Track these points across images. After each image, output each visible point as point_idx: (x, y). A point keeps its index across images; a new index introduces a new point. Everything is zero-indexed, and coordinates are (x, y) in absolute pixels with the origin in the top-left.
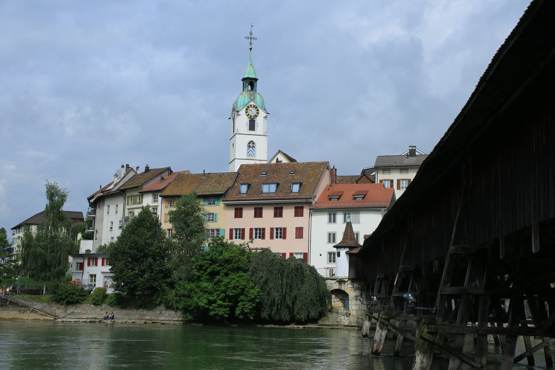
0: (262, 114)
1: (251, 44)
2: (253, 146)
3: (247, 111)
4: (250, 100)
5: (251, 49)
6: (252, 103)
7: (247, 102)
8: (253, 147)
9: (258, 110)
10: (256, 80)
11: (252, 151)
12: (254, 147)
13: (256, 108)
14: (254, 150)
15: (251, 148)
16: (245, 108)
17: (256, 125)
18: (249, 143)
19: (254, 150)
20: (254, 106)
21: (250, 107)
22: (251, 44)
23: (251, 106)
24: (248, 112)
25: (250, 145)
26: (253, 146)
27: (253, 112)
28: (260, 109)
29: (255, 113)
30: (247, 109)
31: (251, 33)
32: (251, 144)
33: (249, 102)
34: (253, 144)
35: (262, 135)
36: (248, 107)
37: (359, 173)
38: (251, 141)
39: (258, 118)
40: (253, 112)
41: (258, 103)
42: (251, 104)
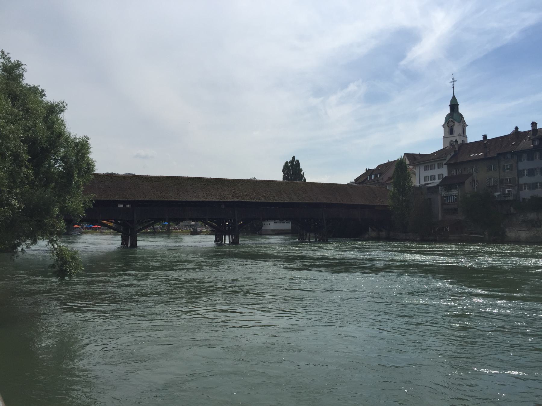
1: (453, 85)
5: (453, 87)
9: (454, 122)
16: (447, 123)
17: (453, 131)
20: (452, 120)
22: (453, 85)
23: (450, 121)
27: (451, 124)
28: (455, 121)
30: (448, 124)
31: (453, 79)
33: (449, 119)
36: (448, 122)
38: (452, 140)
39: (454, 127)
42: (450, 120)
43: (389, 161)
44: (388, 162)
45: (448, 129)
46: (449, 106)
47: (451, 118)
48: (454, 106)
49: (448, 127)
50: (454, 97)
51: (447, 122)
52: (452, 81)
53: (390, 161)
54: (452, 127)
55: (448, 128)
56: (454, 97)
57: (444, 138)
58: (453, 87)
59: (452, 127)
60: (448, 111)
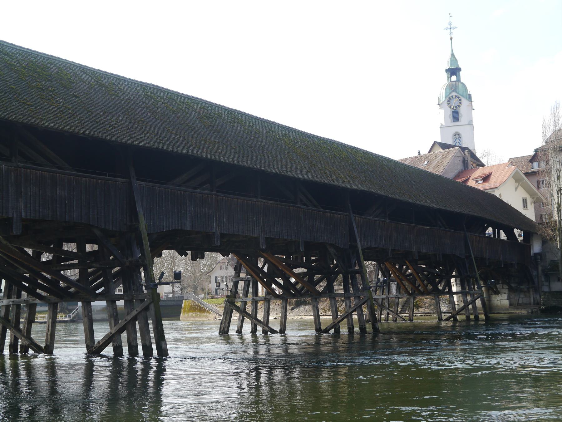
0: (465, 102)
1: (451, 34)
2: (459, 137)
3: (449, 103)
4: (451, 91)
5: (451, 39)
6: (454, 94)
7: (449, 94)
8: (460, 138)
9: (460, 100)
10: (459, 69)
11: (458, 142)
12: (460, 138)
13: (458, 98)
14: (461, 141)
15: (457, 140)
16: (446, 100)
17: (460, 115)
18: (455, 135)
19: (461, 141)
20: (456, 96)
21: (452, 98)
22: (451, 34)
23: (452, 97)
24: (450, 104)
25: (456, 136)
26: (459, 137)
27: (454, 102)
29: (458, 104)
30: (448, 101)
31: (450, 23)
32: (457, 135)
33: (450, 93)
34: (459, 135)
35: (467, 124)
36: (450, 98)
37: (532, 153)
38: (457, 132)
40: (454, 102)
41: (461, 93)
43: (419, 152)
44: (417, 154)
45: (449, 112)
46: (447, 71)
47: (453, 91)
48: (454, 71)
49: (450, 107)
50: (453, 55)
51: (447, 99)
52: (449, 27)
53: (422, 153)
54: (456, 107)
55: (449, 109)
56: (453, 55)
57: (442, 127)
58: (451, 39)
59: (456, 107)
60: (443, 79)
